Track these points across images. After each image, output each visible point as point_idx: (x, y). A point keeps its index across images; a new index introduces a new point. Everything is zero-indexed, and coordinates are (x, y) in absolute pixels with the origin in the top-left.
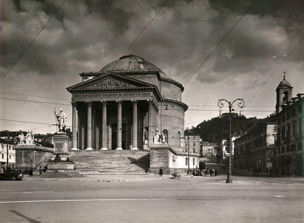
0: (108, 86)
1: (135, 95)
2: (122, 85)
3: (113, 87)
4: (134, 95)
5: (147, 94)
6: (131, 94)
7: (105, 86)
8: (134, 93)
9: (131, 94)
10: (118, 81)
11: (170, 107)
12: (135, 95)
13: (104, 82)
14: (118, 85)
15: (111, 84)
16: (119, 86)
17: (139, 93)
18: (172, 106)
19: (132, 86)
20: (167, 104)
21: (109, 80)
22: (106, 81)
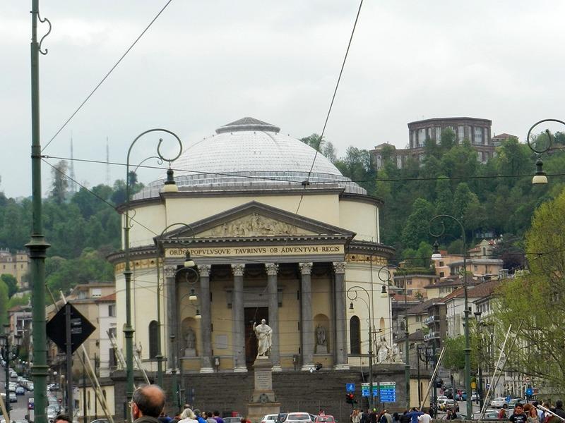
0: (246, 231)
1: (307, 250)
4: (304, 250)
6: (298, 250)
7: (241, 232)
8: (305, 247)
9: (298, 250)
10: (270, 221)
13: (239, 221)
14: (269, 230)
15: (252, 228)
17: (315, 247)
18: (367, 256)
19: (301, 232)
21: (247, 218)
22: (241, 219)
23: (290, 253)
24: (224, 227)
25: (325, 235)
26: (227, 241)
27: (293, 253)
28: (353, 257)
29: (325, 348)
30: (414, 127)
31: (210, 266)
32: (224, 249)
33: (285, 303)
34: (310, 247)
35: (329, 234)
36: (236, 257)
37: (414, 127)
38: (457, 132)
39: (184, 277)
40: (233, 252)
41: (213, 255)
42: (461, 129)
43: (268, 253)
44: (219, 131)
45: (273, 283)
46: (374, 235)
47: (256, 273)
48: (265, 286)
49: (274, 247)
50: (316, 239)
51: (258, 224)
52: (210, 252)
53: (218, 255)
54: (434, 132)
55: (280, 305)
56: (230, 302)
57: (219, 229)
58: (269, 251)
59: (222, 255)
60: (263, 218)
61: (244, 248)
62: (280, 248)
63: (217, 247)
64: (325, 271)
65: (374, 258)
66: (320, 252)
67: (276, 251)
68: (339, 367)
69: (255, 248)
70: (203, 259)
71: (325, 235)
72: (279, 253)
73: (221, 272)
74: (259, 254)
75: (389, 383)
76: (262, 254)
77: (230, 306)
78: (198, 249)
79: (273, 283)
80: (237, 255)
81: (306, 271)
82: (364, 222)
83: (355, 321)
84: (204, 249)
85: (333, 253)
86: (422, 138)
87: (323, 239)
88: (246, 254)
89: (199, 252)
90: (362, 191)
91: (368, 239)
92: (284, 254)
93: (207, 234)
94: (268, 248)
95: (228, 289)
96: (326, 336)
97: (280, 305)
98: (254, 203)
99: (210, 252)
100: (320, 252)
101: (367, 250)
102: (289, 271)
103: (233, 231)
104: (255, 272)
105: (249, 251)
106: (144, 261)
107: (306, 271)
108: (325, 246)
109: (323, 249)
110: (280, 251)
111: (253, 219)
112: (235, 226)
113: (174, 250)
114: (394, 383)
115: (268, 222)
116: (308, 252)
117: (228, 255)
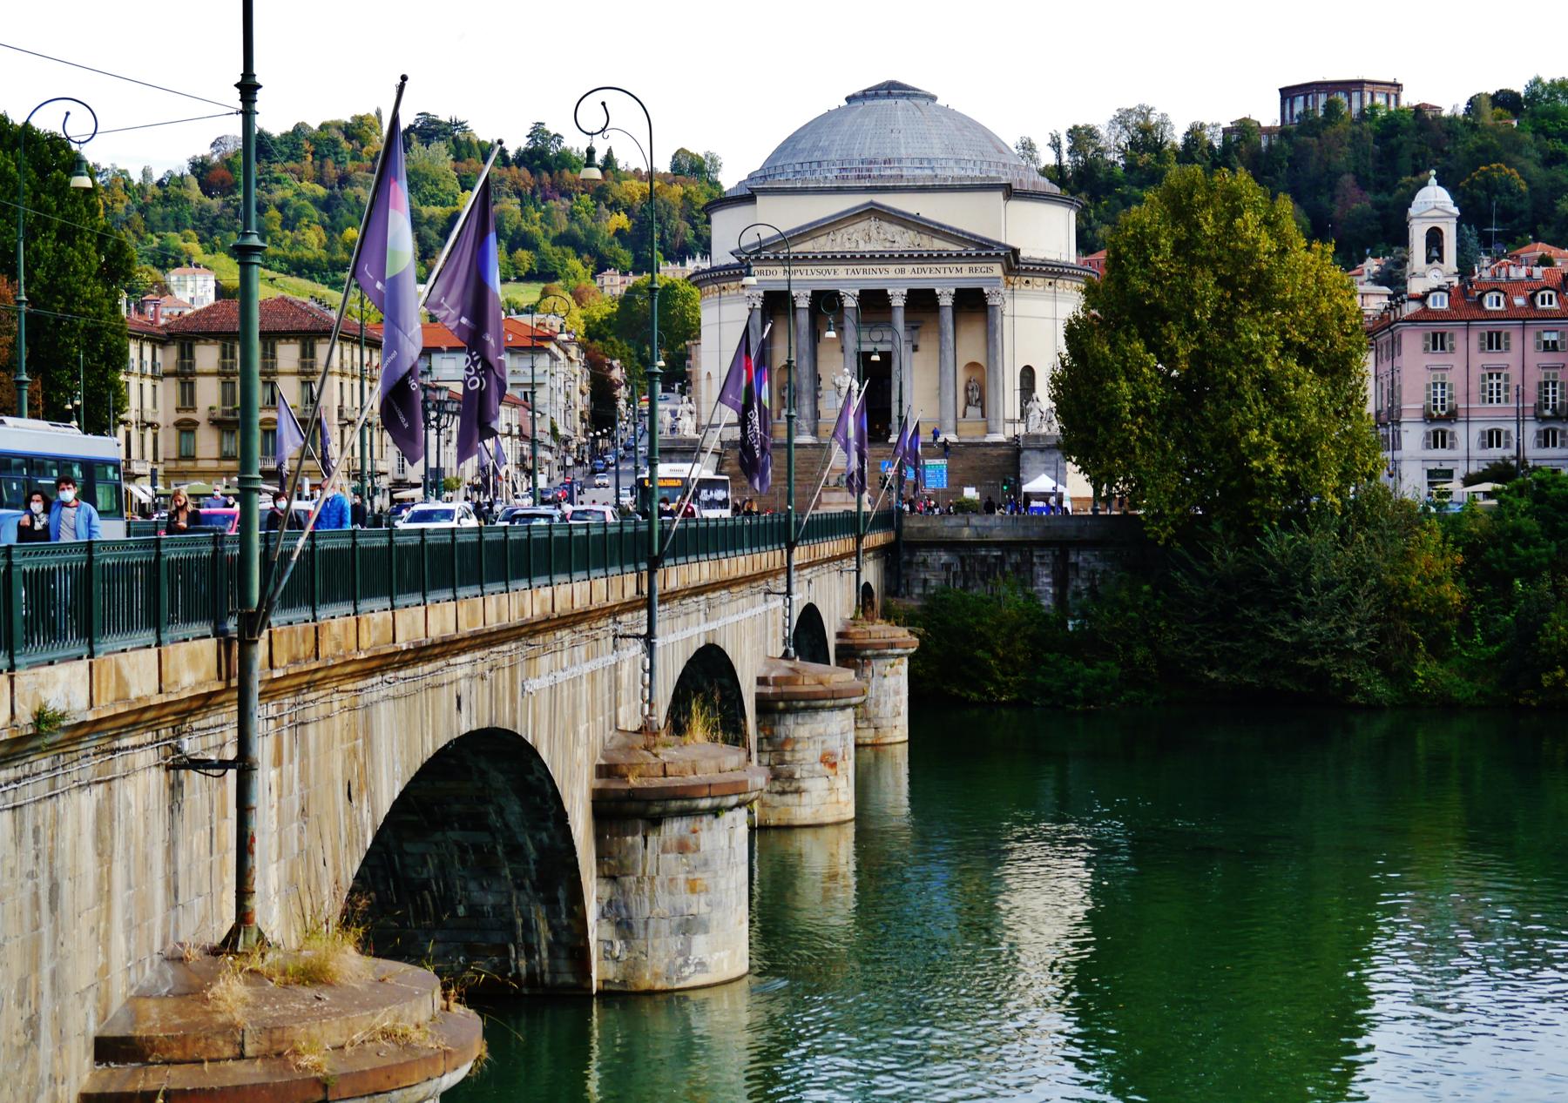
0: (861, 243)
2: (905, 240)
3: (875, 246)
13: (851, 229)
19: (939, 245)
21: (863, 225)
23: (923, 275)
25: (973, 250)
26: (834, 257)
27: (928, 275)
29: (979, 411)
30: (1287, 94)
31: (809, 293)
33: (922, 345)
35: (983, 250)
36: (848, 281)
37: (1287, 94)
38: (1350, 101)
39: (776, 304)
40: (842, 272)
41: (815, 277)
42: (1356, 96)
43: (892, 275)
44: (848, 99)
45: (899, 318)
46: (1064, 251)
48: (889, 324)
50: (959, 256)
54: (1315, 100)
55: (915, 349)
57: (822, 240)
58: (892, 271)
60: (885, 225)
62: (908, 268)
64: (972, 303)
65: (1059, 282)
67: (903, 271)
68: (991, 438)
70: (804, 282)
71: (973, 250)
72: (908, 275)
73: (826, 303)
74: (878, 276)
75: (937, 462)
76: (883, 276)
79: (899, 318)
81: (946, 301)
82: (1049, 232)
83: (1028, 374)
86: (1299, 107)
87: (969, 255)
88: (861, 276)
90: (1056, 189)
91: (1052, 256)
93: (806, 247)
94: (892, 268)
96: (979, 394)
97: (915, 349)
98: (872, 203)
100: (966, 274)
101: (1052, 271)
102: (922, 302)
103: (842, 243)
104: (874, 303)
106: (733, 284)
107: (946, 301)
110: (909, 270)
111: (871, 225)
114: (943, 462)
115: (892, 230)
116: (948, 274)
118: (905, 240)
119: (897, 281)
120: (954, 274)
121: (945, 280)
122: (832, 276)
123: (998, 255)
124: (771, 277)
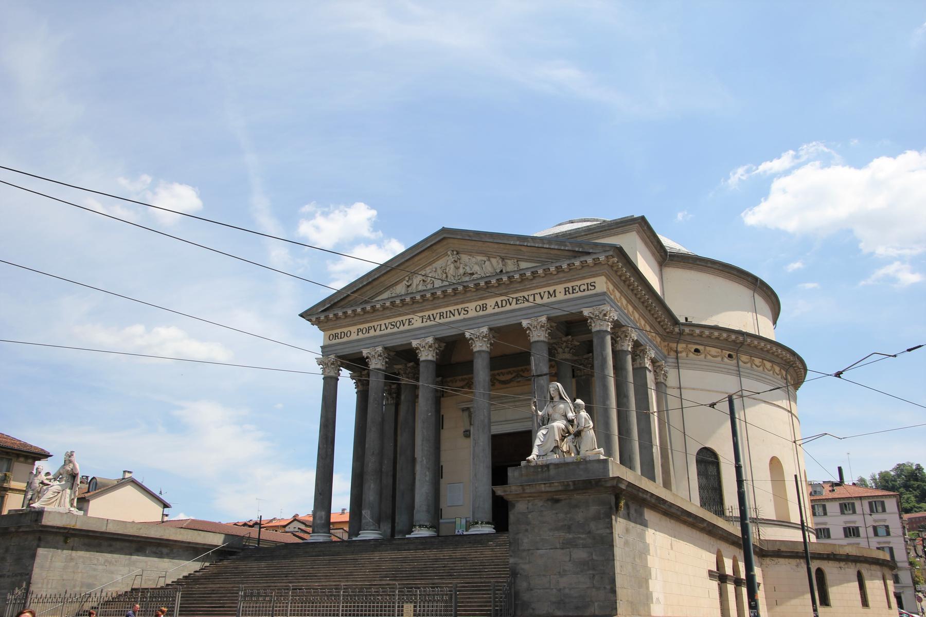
1: (537, 297)
5: (582, 288)
11: (719, 359)
12: (537, 297)
13: (428, 270)
14: (473, 274)
16: (475, 276)
17: (551, 289)
20: (700, 348)
21: (440, 263)
22: (434, 265)
23: (508, 307)
24: (405, 282)
27: (514, 306)
28: (697, 351)
32: (404, 318)
34: (541, 290)
41: (389, 331)
43: (472, 314)
47: (509, 377)
49: (480, 303)
51: (457, 268)
52: (383, 327)
53: (396, 329)
56: (468, 428)
58: (472, 309)
59: (402, 328)
60: (465, 258)
61: (434, 312)
62: (491, 302)
63: (395, 316)
66: (558, 296)
67: (484, 307)
69: (451, 309)
72: (490, 310)
74: (457, 317)
76: (462, 317)
77: (467, 434)
78: (366, 325)
80: (423, 325)
84: (375, 324)
85: (586, 293)
89: (368, 330)
92: (497, 310)
94: (472, 306)
95: (465, 406)
99: (383, 327)
100: (560, 296)
105: (441, 315)
108: (569, 285)
109: (566, 291)
112: (420, 278)
113: (334, 332)
117: (410, 327)
118: (481, 266)
119: (476, 319)
120: (546, 300)
121: (534, 308)
122: (407, 327)
123: (597, 263)
124: (345, 339)
